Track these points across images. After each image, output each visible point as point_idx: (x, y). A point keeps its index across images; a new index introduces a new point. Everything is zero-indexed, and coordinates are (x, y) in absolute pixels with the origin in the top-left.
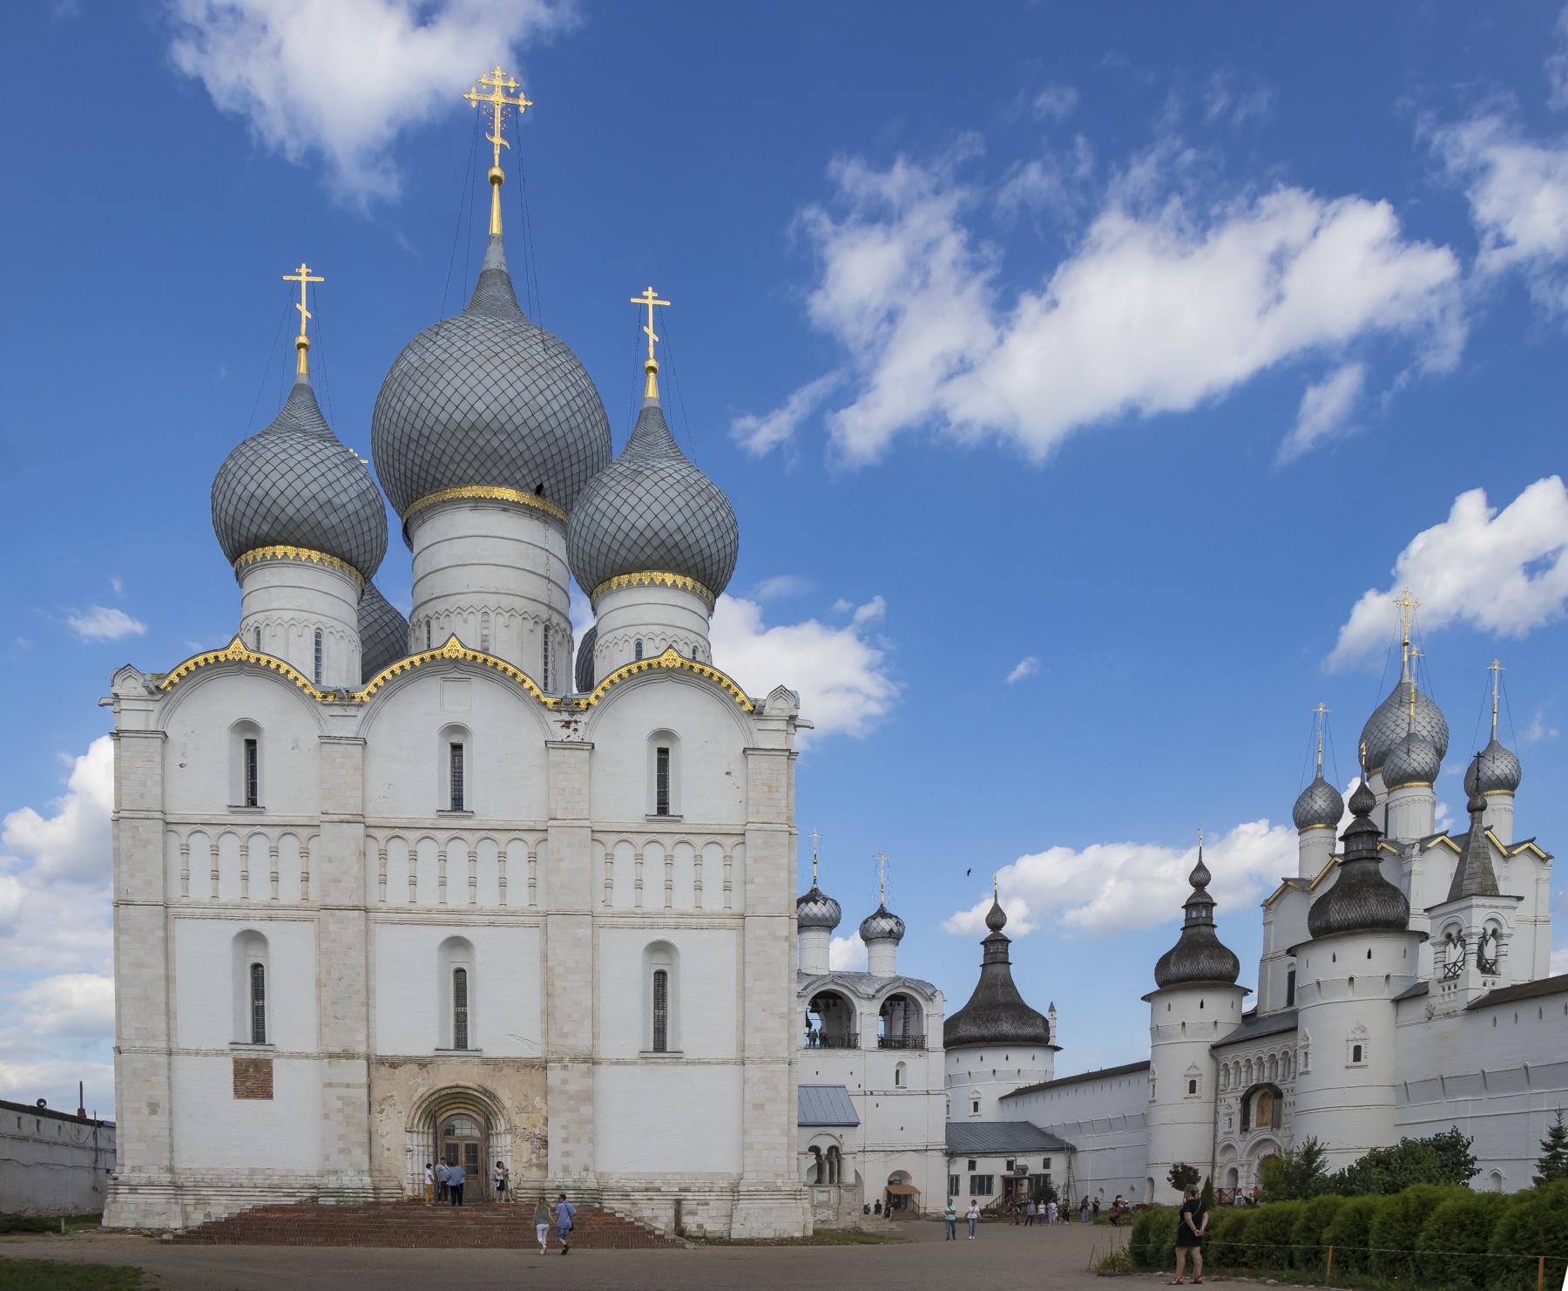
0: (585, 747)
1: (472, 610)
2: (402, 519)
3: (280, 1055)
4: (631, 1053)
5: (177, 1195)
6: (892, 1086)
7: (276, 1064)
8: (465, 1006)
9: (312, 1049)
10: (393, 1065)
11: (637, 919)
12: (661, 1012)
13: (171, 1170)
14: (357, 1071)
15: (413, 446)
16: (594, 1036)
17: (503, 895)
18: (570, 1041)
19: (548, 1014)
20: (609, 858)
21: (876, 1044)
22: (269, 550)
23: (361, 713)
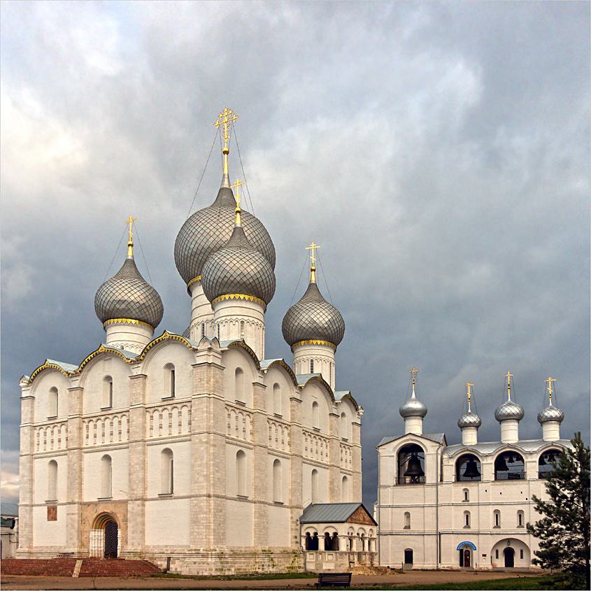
7: (59, 507)
10: (89, 505)
14: (75, 508)
15: (192, 258)
17: (120, 437)
19: (130, 481)
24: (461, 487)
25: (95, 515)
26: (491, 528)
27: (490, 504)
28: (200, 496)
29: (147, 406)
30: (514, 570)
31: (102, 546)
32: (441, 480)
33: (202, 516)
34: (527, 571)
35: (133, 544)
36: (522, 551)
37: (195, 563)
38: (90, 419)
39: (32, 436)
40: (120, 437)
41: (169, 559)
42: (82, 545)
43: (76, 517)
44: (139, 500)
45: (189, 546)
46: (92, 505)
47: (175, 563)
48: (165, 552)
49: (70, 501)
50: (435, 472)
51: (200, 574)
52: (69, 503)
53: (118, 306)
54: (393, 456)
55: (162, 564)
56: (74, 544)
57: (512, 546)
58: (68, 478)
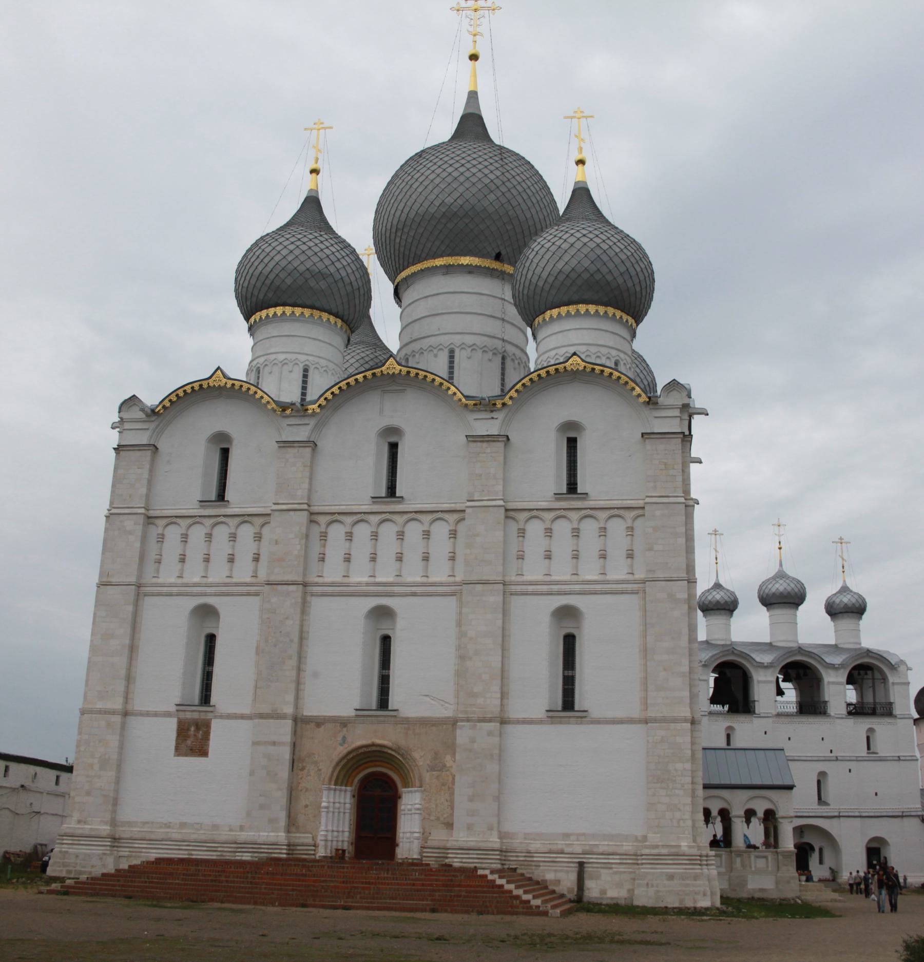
0: (500, 439)
1: (441, 347)
2: (394, 284)
3: (221, 717)
4: (539, 712)
5: (114, 847)
6: (863, 752)
7: (217, 727)
8: (389, 669)
9: (247, 711)
11: (548, 588)
12: (570, 673)
13: (113, 823)
14: (284, 730)
16: (504, 695)
18: (480, 701)
19: (460, 674)
20: (522, 533)
21: (844, 712)
22: (271, 311)
23: (312, 422)
25: (342, 750)
28: (674, 720)
29: (511, 506)
31: (347, 829)
33: (679, 766)
35: (470, 827)
36: (821, 850)
37: (671, 877)
38: (335, 517)
39: (144, 539)
40: (426, 568)
41: (581, 865)
42: (292, 823)
43: (286, 753)
44: (490, 720)
45: (645, 838)
46: (330, 726)
47: (598, 877)
48: (567, 850)
49: (265, 709)
51: (689, 904)
52: (262, 716)
53: (312, 283)
55: (566, 881)
56: (272, 821)
57: (807, 839)
58: (258, 651)
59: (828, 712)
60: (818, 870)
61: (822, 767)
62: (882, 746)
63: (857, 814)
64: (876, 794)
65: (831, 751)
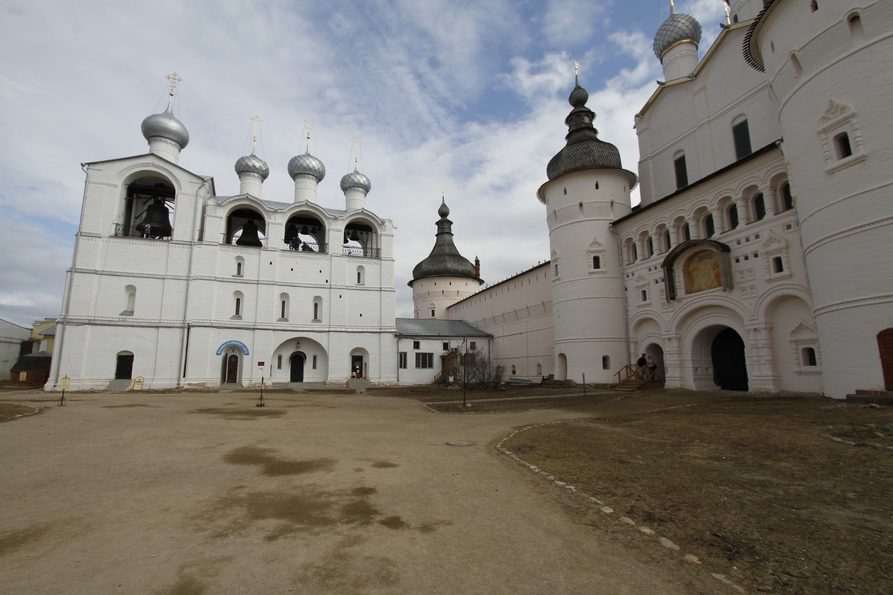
24: (234, 252)
26: (274, 320)
27: (274, 284)
30: (306, 387)
32: (201, 239)
34: (323, 387)
36: (315, 358)
50: (190, 224)
54: (116, 186)
57: (301, 350)
59: (327, 251)
60: (310, 375)
61: (318, 292)
62: (370, 279)
63: (343, 330)
64: (361, 315)
65: (327, 281)
